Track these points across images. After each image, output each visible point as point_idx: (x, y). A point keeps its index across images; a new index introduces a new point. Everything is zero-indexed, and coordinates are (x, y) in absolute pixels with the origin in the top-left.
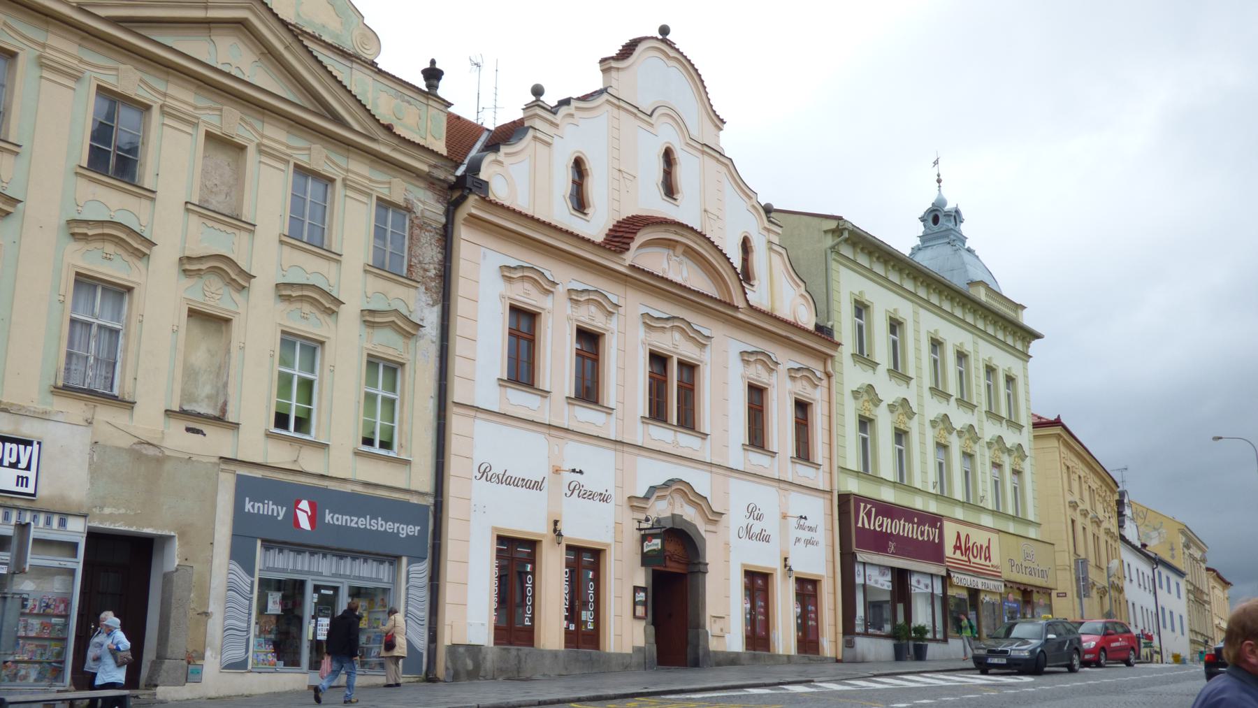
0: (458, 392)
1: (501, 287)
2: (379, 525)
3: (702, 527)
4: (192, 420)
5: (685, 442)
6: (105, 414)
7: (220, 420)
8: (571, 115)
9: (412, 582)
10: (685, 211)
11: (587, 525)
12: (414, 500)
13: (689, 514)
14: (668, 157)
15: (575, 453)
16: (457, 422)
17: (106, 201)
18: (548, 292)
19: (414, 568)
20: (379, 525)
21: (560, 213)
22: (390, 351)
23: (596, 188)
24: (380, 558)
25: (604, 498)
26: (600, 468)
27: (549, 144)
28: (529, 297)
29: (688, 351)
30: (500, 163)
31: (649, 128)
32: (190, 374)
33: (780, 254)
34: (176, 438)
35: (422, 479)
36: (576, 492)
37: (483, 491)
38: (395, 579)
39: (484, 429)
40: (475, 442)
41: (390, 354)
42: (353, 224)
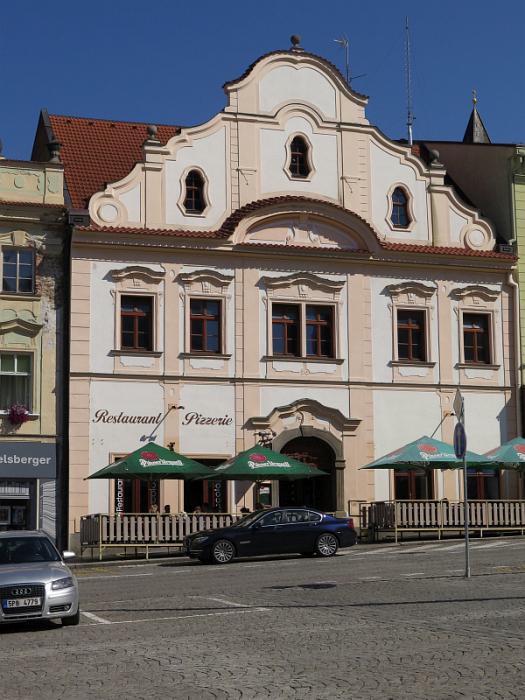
0: (75, 366)
2: (16, 460)
5: (320, 369)
8: (184, 141)
9: (45, 494)
10: (320, 186)
11: (220, 443)
12: (45, 441)
13: (322, 425)
14: (299, 146)
15: (187, 394)
16: (75, 385)
18: (157, 282)
19: (44, 486)
20: (16, 460)
21: (172, 217)
22: (19, 346)
23: (213, 192)
24: (20, 482)
25: (223, 422)
26: (217, 400)
27: (159, 170)
29: (319, 297)
30: (110, 196)
31: (274, 126)
33: (447, 193)
35: (48, 425)
36: (194, 420)
37: (98, 429)
38: (33, 493)
41: (19, 348)
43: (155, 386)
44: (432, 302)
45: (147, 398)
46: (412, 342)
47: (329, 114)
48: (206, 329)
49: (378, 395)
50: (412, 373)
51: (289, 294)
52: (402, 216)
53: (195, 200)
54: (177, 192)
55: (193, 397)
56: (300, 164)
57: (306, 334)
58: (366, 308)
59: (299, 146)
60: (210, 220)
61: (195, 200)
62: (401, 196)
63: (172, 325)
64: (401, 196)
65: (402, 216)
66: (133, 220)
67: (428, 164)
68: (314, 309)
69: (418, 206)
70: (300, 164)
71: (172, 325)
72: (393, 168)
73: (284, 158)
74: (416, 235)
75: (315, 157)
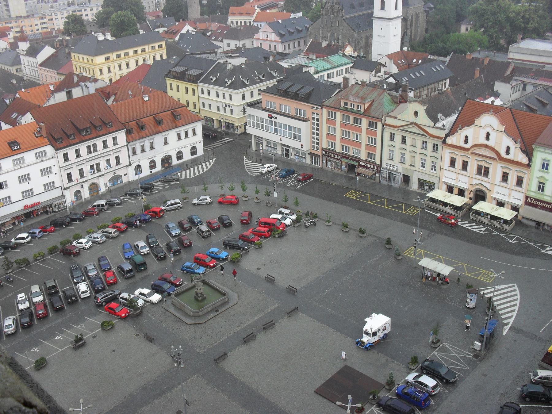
1: (449, 154)
3: (487, 191)
4: (411, 165)
5: (485, 179)
6: (403, 165)
7: (414, 166)
10: (490, 143)
13: (484, 189)
14: (488, 134)
15: (460, 176)
17: (403, 146)
26: (466, 179)
28: (453, 156)
29: (487, 166)
32: (412, 161)
34: (410, 167)
39: (445, 171)
40: (445, 173)
42: (430, 146)
43: (455, 174)
44: (511, 172)
45: (453, 176)
46: (505, 177)
47: (495, 128)
48: (465, 166)
49: (496, 187)
50: (504, 184)
51: (480, 164)
52: (508, 152)
53: (466, 141)
54: (463, 139)
55: (461, 178)
56: (488, 138)
57: (484, 171)
58: (496, 170)
59: (488, 134)
60: (468, 146)
61: (466, 141)
62: (508, 149)
63: (459, 164)
64: (508, 149)
65: (508, 152)
66: (454, 143)
67: (515, 142)
68: (485, 167)
69: (511, 151)
70: (488, 138)
71: (459, 164)
72: (507, 141)
73: (485, 135)
74: (510, 157)
75: (490, 137)
